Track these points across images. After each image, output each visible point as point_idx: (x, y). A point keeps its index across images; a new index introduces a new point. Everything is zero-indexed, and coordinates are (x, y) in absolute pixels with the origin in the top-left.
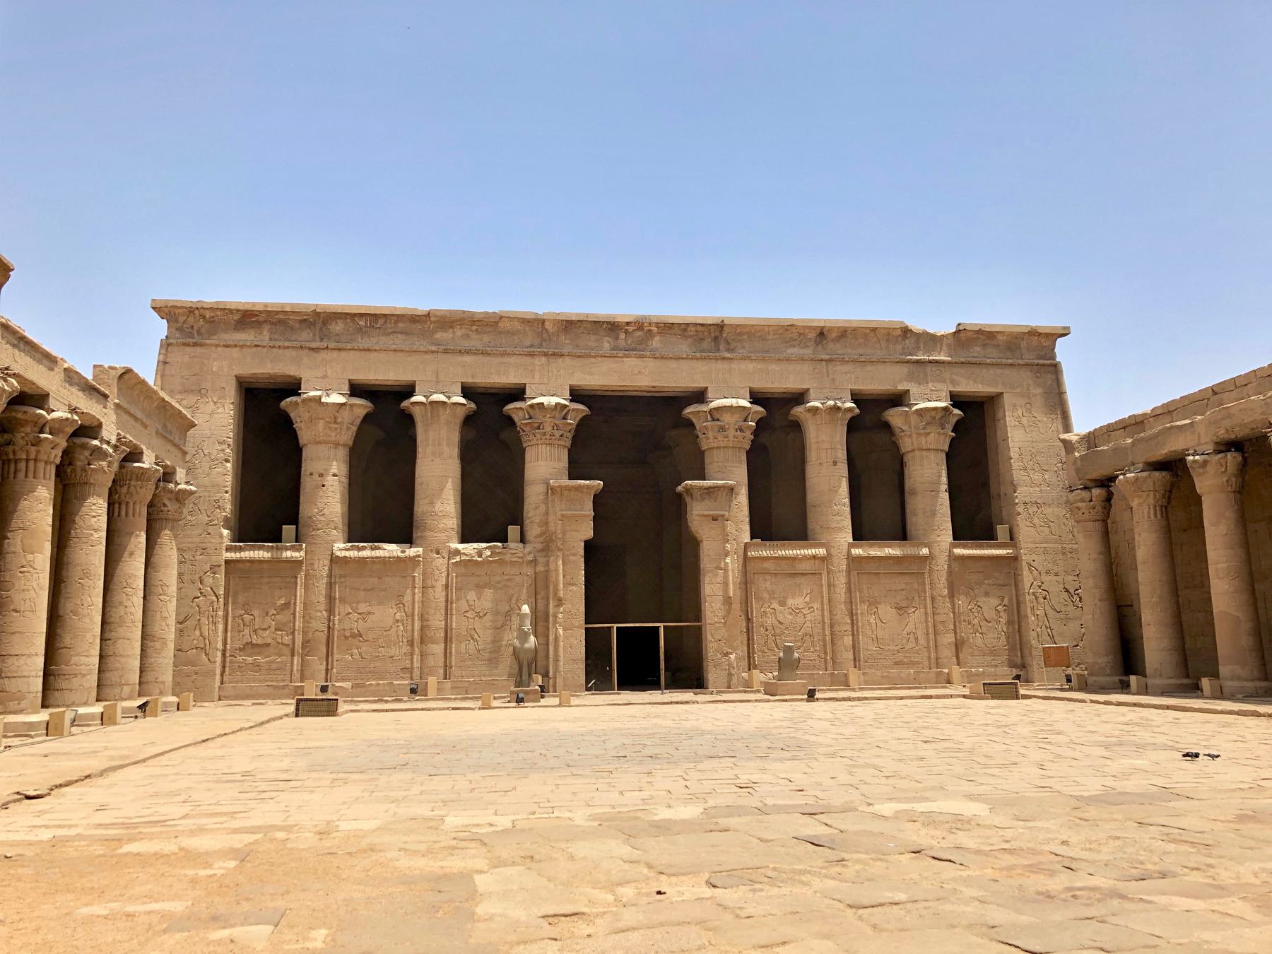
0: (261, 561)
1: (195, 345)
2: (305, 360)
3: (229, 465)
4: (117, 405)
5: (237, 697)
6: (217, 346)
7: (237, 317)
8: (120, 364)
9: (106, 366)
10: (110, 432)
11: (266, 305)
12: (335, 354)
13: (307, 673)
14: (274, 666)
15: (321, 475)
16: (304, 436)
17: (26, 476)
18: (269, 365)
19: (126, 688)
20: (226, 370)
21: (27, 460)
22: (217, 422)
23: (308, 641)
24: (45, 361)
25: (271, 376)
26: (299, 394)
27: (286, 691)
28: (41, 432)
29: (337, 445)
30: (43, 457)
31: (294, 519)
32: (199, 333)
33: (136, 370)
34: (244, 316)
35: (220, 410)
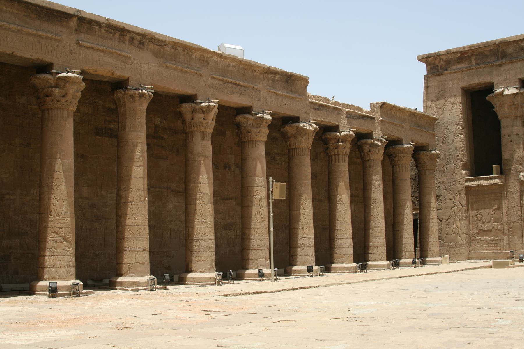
0: (483, 186)
1: (439, 75)
2: (495, 72)
3: (462, 136)
4: (381, 121)
5: (477, 258)
6: (450, 73)
7: (459, 55)
8: (380, 100)
9: (375, 103)
10: (378, 134)
11: (470, 47)
12: (510, 66)
13: (512, 245)
14: (495, 242)
15: (509, 136)
16: (500, 115)
17: (335, 162)
18: (477, 79)
19: (407, 253)
20: (456, 85)
21: (335, 155)
22: (453, 113)
23: (511, 228)
24: (334, 111)
25: (478, 85)
26: (494, 92)
27: (501, 255)
28: (338, 142)
29: (517, 117)
30: (340, 153)
31: (499, 160)
32: (441, 67)
33: (388, 102)
34: (461, 55)
35: (455, 108)
